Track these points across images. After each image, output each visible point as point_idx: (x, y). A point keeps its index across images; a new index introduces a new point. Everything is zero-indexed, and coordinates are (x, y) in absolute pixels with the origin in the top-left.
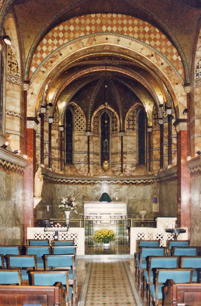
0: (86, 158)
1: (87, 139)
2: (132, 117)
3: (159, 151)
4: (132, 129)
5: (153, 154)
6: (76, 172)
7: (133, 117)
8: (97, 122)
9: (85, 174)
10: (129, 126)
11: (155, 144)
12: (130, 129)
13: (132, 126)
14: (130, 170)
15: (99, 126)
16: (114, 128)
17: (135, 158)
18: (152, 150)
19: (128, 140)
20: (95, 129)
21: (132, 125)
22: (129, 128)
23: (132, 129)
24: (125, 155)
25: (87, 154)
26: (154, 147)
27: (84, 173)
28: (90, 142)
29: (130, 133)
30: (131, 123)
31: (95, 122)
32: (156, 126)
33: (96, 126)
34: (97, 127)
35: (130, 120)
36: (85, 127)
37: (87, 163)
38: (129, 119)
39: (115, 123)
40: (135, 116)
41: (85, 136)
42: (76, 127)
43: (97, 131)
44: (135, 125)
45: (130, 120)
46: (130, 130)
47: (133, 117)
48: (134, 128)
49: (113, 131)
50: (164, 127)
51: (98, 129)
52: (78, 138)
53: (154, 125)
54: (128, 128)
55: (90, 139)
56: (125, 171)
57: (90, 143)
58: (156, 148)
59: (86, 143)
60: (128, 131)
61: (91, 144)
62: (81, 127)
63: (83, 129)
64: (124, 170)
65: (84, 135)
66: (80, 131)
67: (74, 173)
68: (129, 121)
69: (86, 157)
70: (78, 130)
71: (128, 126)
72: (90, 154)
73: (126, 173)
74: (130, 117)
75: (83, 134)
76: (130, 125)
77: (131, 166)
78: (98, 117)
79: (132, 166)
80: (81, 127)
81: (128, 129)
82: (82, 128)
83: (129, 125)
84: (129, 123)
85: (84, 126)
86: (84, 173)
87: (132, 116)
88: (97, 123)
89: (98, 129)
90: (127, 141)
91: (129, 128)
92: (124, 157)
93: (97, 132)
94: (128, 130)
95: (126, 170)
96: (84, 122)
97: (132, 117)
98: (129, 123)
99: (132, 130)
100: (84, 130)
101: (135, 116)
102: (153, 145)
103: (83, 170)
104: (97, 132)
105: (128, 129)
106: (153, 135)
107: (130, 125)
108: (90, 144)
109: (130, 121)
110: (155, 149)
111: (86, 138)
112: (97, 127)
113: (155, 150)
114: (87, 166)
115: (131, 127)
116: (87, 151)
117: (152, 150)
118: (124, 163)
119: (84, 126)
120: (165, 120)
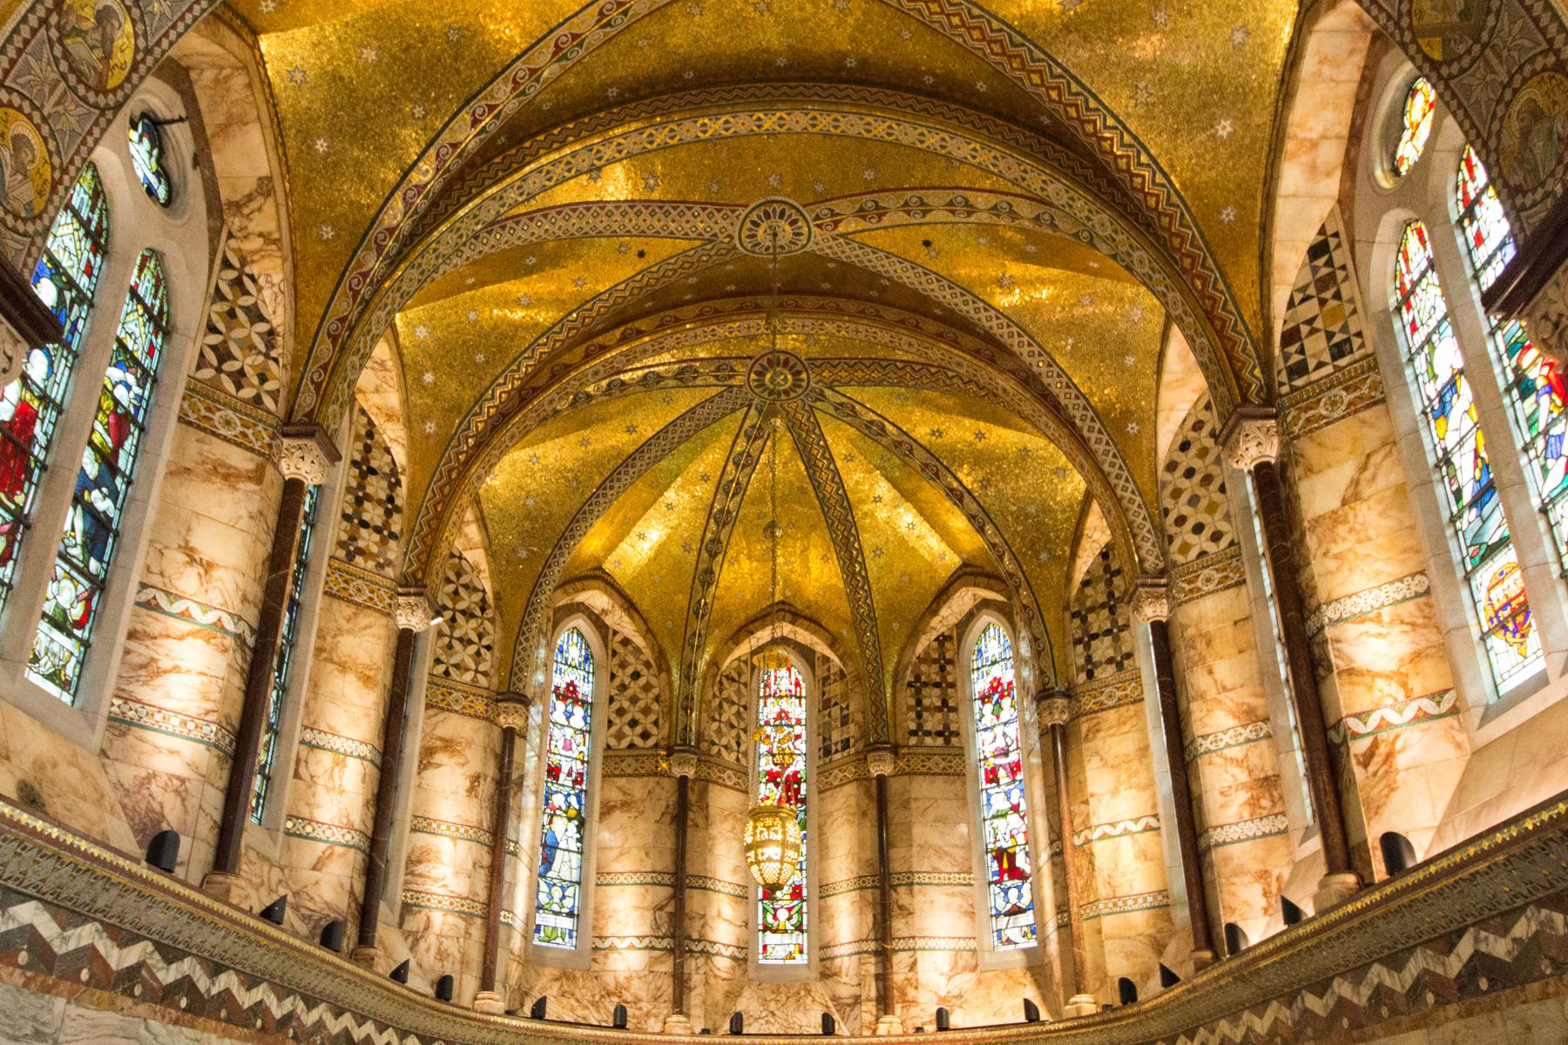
0: (663, 915)
1: (674, 798)
2: (935, 667)
3: (1135, 841)
4: (939, 734)
5: (1091, 863)
6: (593, 1003)
7: (942, 669)
8: (733, 703)
9: (652, 1022)
10: (919, 716)
11: (1106, 798)
12: (928, 733)
13: (939, 716)
14: (943, 994)
15: (745, 731)
16: (836, 736)
17: (966, 913)
18: (1088, 841)
19: (916, 799)
20: (724, 741)
21: (939, 709)
22: (920, 726)
23: (939, 734)
24: (902, 890)
25: (670, 891)
26: (1094, 821)
27: (648, 1015)
28: (691, 815)
29: (929, 757)
30: (932, 697)
31: (725, 705)
32: (1095, 685)
33: (732, 726)
34: (734, 733)
35: (925, 684)
36: (665, 732)
37: (665, 949)
38: (917, 678)
39: (835, 711)
40: (951, 662)
41: (665, 781)
42: (614, 729)
43: (734, 755)
44: (954, 710)
45: (925, 684)
46: (928, 741)
47: (942, 669)
48: (953, 727)
49: (827, 752)
50: (1191, 632)
51: (738, 744)
52: (620, 789)
53: (1083, 677)
54: (913, 726)
55: (692, 797)
56: (908, 1003)
57: (690, 823)
58: (1113, 825)
59: (668, 818)
60: (916, 746)
61: (697, 826)
62: (639, 729)
63: (651, 742)
64: (903, 993)
65: (656, 774)
66: (637, 752)
67: (580, 1012)
68: (918, 691)
69: (661, 908)
70: (625, 743)
71: (912, 715)
72: (688, 892)
73: (914, 1011)
74: (924, 668)
75: (649, 765)
76: (927, 709)
77: (946, 968)
78: (743, 679)
79: (954, 967)
80: (639, 729)
81: (914, 733)
82: (645, 735)
83: (919, 709)
84: (919, 703)
85: (656, 723)
86: (648, 1015)
87: (935, 661)
88: (738, 714)
89: (738, 744)
90: (913, 805)
91: (920, 726)
92: (901, 907)
93: (738, 759)
94: (913, 741)
95: (911, 993)
96: (657, 699)
97: (935, 667)
98: (919, 703)
99: (940, 741)
100: (656, 746)
101: (951, 662)
102: (1086, 802)
103: (643, 995)
104: (738, 759)
105: (914, 733)
106: (1086, 738)
107: (927, 709)
108: (689, 830)
109: (925, 691)
110: (1109, 830)
111: (666, 794)
112: (734, 733)
113: (1104, 837)
114: (667, 966)
115: (932, 722)
116: (671, 869)
117: (1088, 841)
118: (901, 944)
119: (656, 723)
120: (1187, 587)
